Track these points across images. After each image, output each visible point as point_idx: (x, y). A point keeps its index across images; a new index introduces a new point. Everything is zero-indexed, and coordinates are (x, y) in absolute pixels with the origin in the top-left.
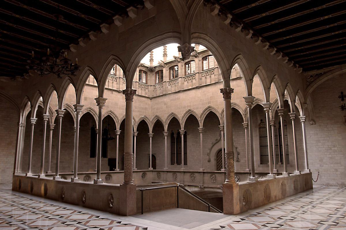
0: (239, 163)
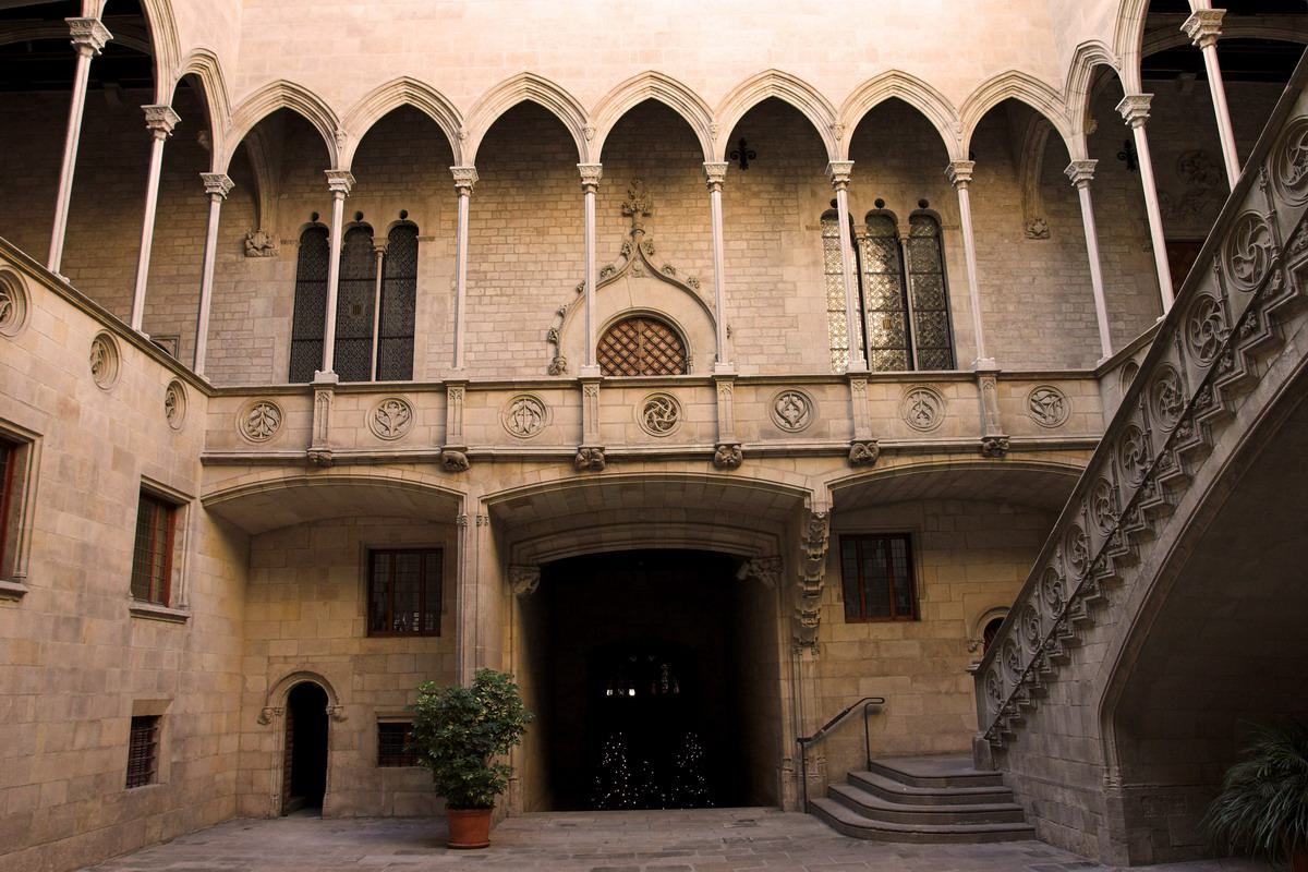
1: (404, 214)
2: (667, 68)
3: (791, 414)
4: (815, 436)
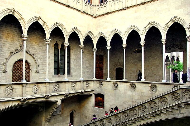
0: (38, 74)
3: (56, 87)
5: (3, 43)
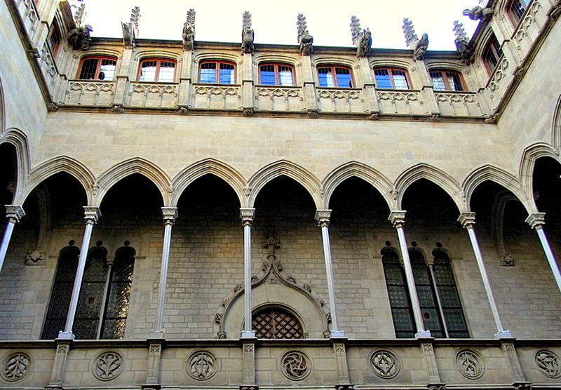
1: (127, 243)
2: (292, 158)
3: (384, 366)
4: (402, 382)
5: (216, 267)
